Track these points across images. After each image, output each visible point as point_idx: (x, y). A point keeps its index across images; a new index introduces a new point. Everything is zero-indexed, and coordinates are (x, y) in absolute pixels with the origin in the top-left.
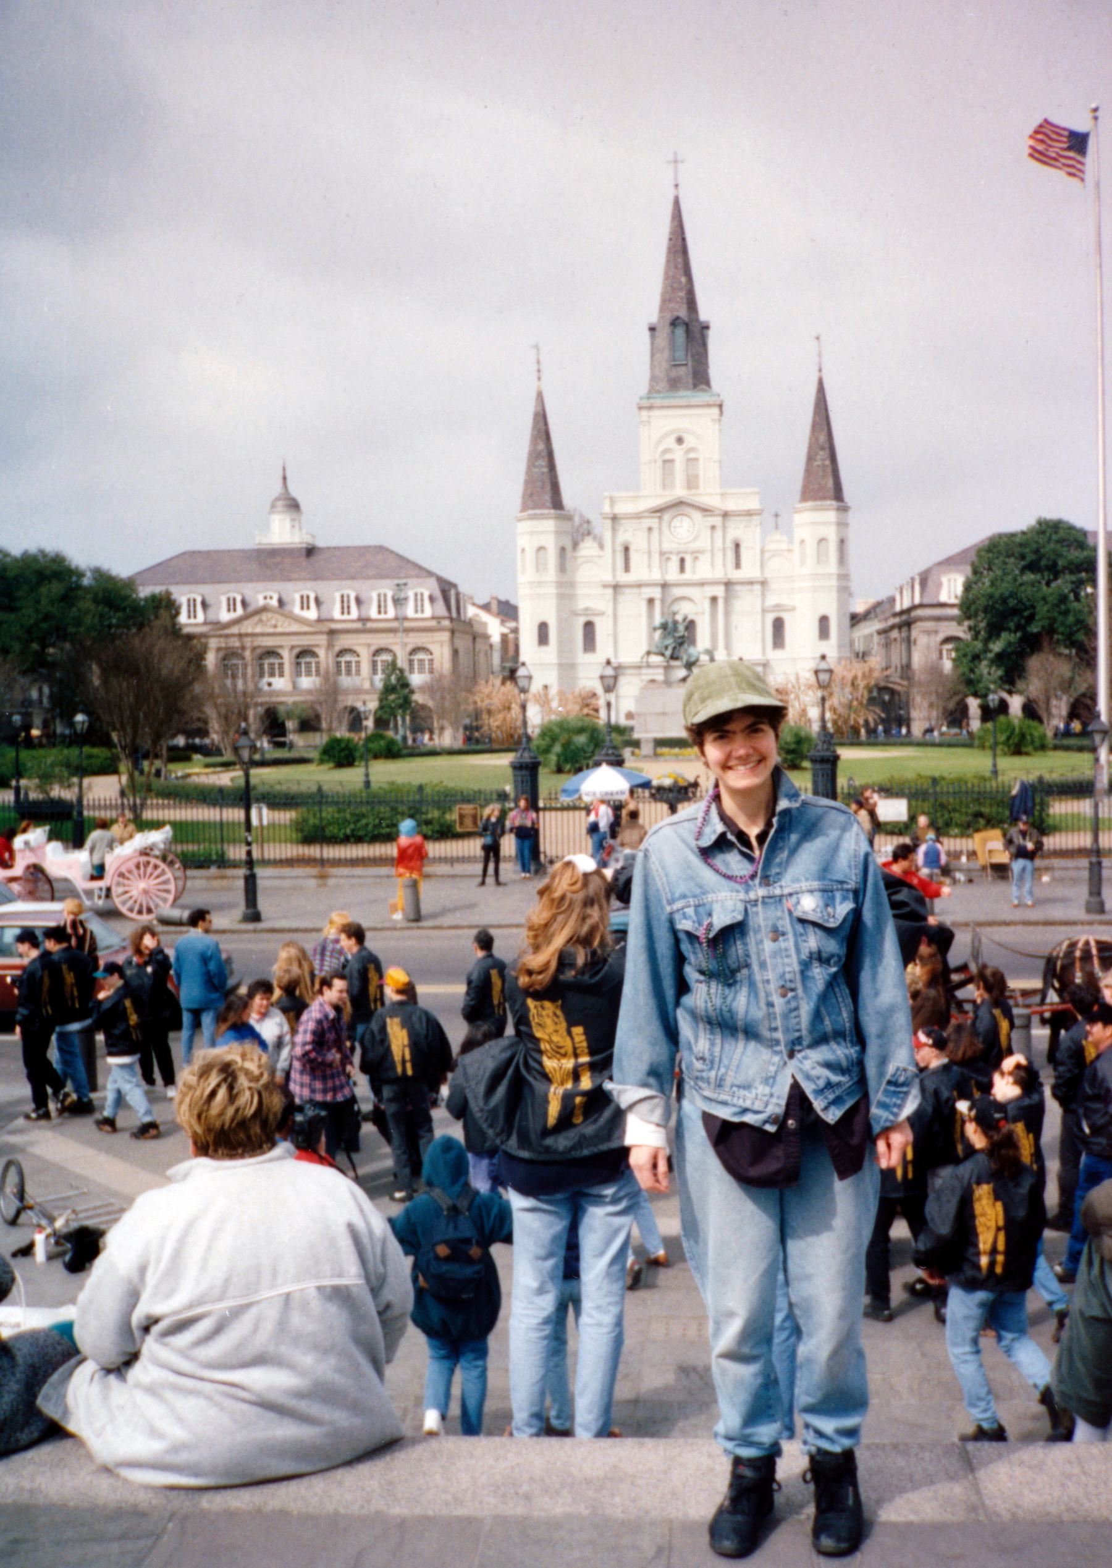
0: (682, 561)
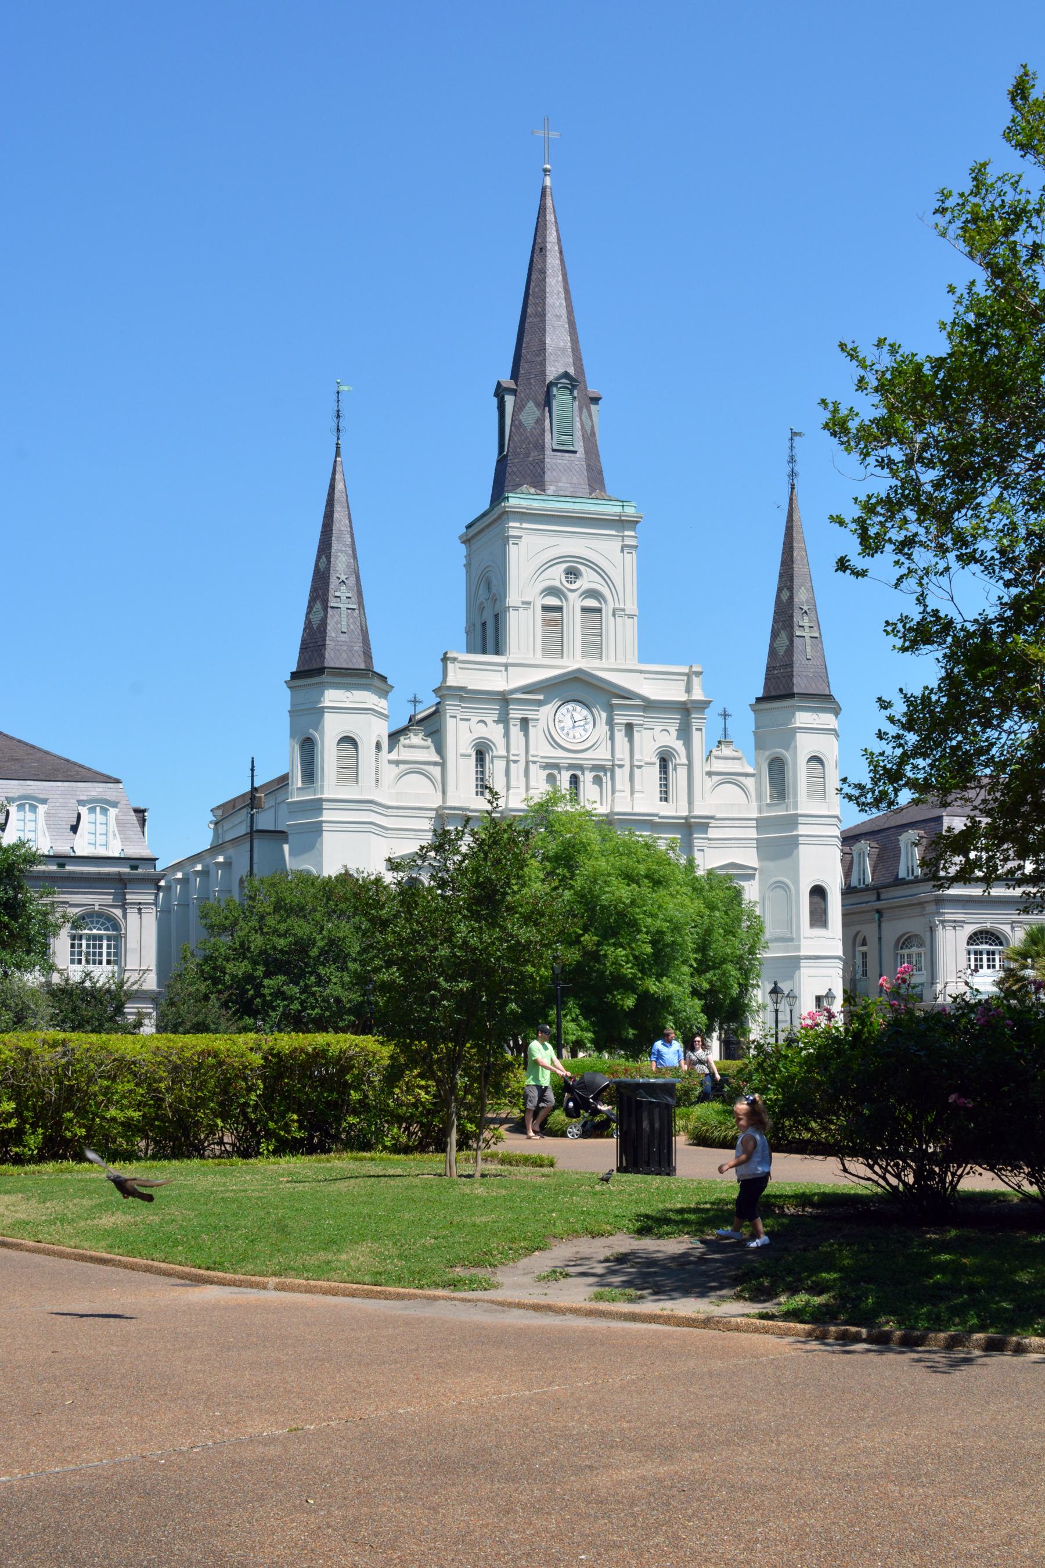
0: (574, 780)
